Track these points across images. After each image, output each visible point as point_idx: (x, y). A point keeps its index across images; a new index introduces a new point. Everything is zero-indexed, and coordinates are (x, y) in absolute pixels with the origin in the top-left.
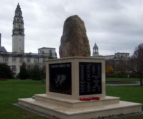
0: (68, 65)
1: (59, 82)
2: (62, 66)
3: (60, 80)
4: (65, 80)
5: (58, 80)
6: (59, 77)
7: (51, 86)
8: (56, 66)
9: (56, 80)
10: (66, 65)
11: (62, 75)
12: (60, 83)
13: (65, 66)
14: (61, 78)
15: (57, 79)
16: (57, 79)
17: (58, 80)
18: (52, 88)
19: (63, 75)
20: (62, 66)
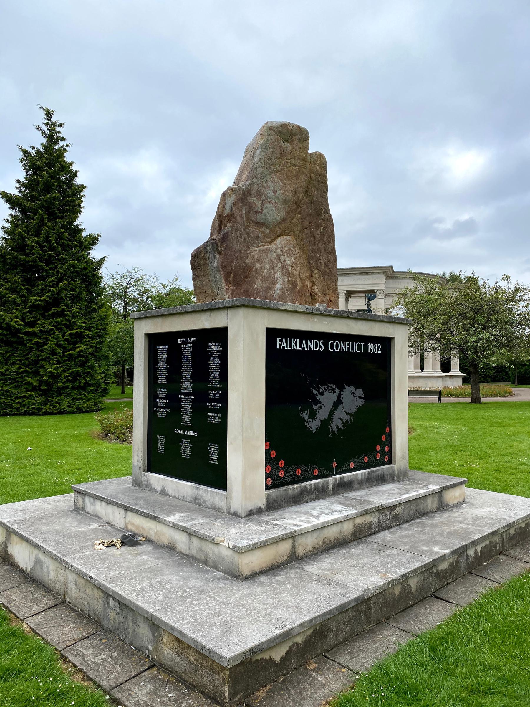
0: (374, 348)
1: (326, 423)
2: (345, 349)
3: (332, 413)
4: (359, 408)
5: (323, 414)
6: (327, 399)
7: (273, 454)
8: (316, 346)
9: (313, 415)
10: (366, 347)
11: (342, 388)
12: (336, 424)
13: (359, 347)
14: (338, 403)
15: (315, 407)
16: (315, 407)
17: (323, 414)
18: (282, 463)
19: (348, 391)
20: (344, 347)
